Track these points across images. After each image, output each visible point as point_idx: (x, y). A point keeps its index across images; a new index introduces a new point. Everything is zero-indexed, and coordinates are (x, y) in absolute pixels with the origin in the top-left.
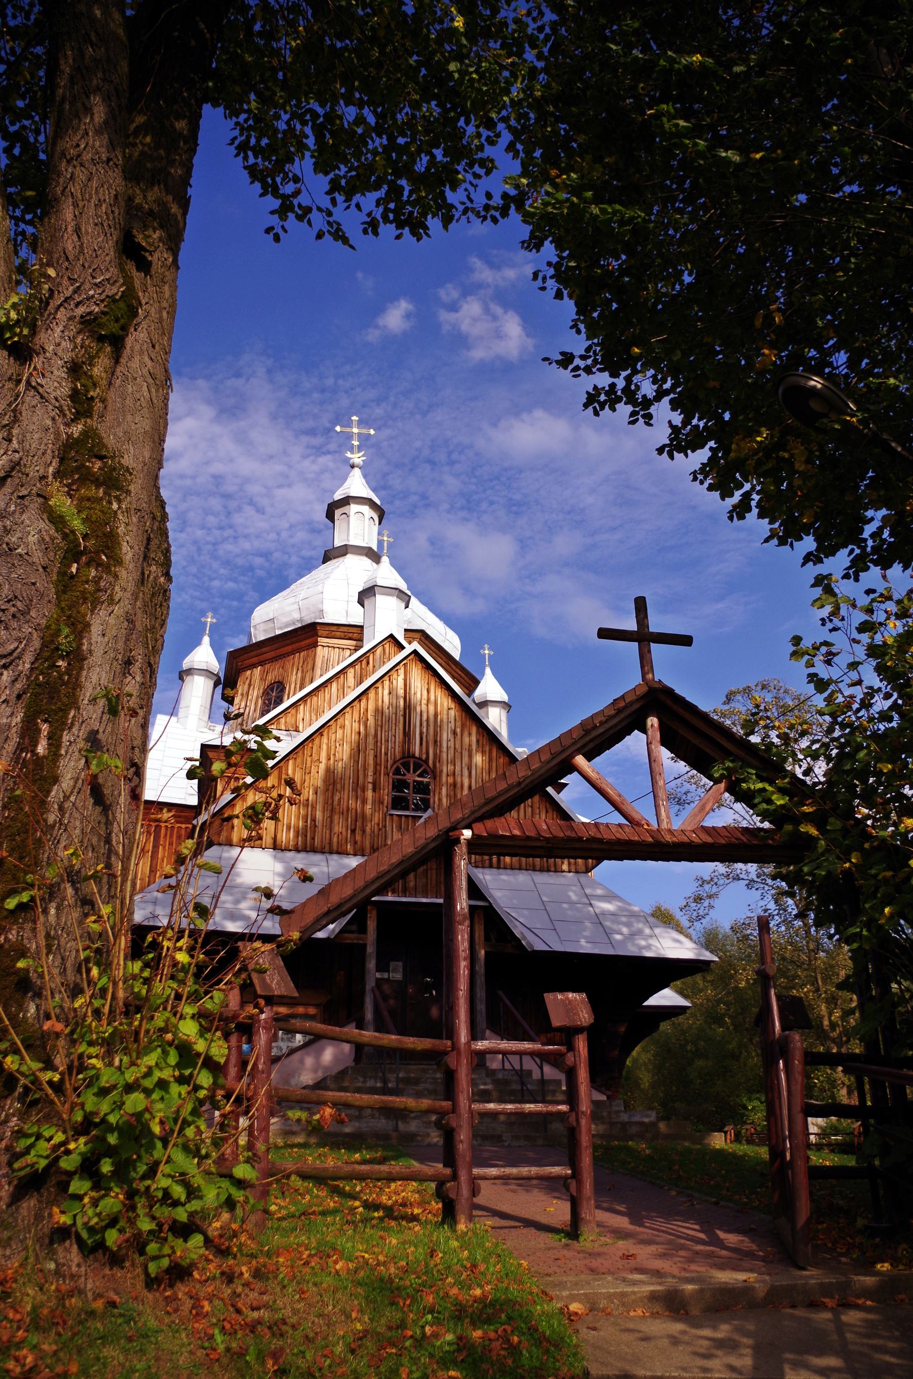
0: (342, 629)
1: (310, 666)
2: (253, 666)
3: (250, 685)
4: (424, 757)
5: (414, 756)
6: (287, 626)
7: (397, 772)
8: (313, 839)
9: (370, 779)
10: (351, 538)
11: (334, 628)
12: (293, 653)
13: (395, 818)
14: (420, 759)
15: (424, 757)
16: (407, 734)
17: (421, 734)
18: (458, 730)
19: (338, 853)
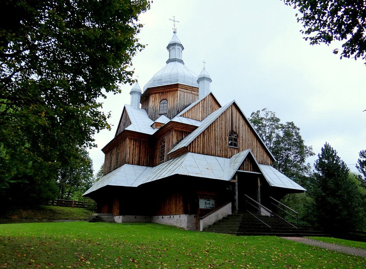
0: (185, 86)
1: (176, 96)
2: (155, 93)
3: (155, 99)
4: (236, 132)
5: (233, 131)
6: (166, 82)
7: (230, 135)
8: (212, 152)
9: (224, 137)
10: (176, 56)
11: (183, 86)
12: (169, 91)
13: (230, 148)
14: (235, 132)
15: (236, 132)
16: (232, 125)
17: (235, 125)
18: (243, 125)
19: (217, 156)
